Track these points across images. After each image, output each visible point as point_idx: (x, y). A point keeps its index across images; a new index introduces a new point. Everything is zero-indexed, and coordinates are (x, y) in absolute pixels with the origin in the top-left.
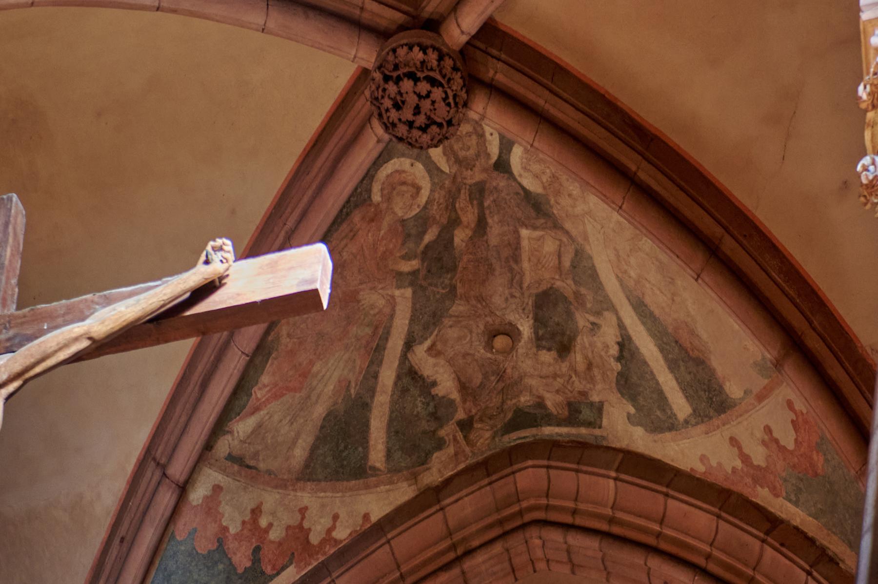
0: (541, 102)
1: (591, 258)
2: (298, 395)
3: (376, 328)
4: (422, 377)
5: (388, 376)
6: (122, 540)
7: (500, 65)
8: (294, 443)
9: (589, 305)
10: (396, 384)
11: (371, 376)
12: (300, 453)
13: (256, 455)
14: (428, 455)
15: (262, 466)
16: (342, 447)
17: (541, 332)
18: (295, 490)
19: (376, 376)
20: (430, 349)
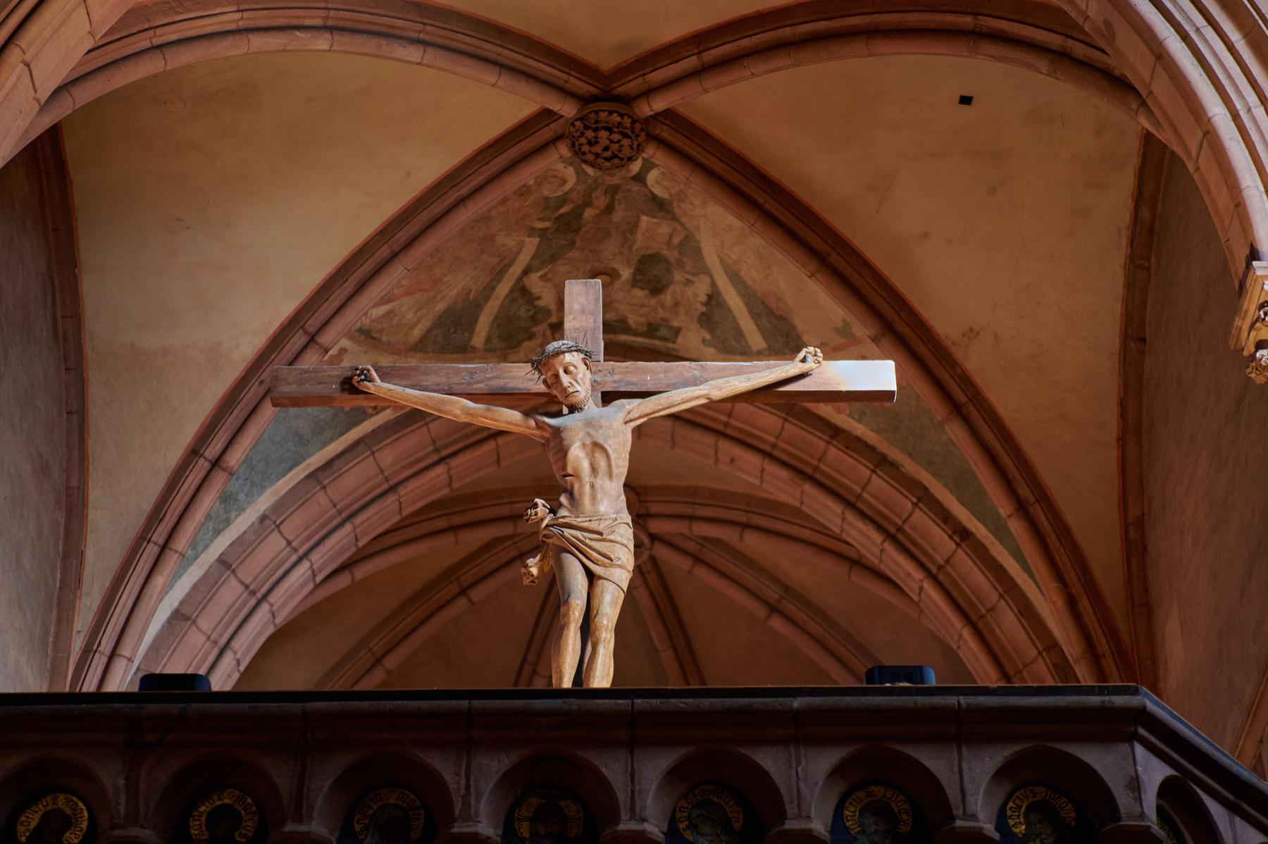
0: (694, 153)
1: (698, 242)
2: (427, 294)
3: (503, 259)
4: (530, 294)
5: (503, 289)
6: (262, 382)
7: (665, 128)
8: (415, 325)
9: (687, 268)
10: (508, 295)
11: (489, 290)
12: (417, 333)
13: (381, 331)
14: (519, 343)
15: (384, 338)
16: (452, 330)
17: (638, 278)
18: (406, 357)
19: (493, 289)
20: (542, 277)
